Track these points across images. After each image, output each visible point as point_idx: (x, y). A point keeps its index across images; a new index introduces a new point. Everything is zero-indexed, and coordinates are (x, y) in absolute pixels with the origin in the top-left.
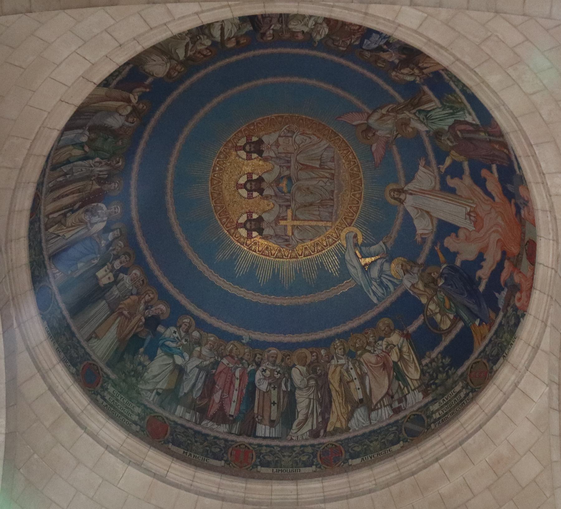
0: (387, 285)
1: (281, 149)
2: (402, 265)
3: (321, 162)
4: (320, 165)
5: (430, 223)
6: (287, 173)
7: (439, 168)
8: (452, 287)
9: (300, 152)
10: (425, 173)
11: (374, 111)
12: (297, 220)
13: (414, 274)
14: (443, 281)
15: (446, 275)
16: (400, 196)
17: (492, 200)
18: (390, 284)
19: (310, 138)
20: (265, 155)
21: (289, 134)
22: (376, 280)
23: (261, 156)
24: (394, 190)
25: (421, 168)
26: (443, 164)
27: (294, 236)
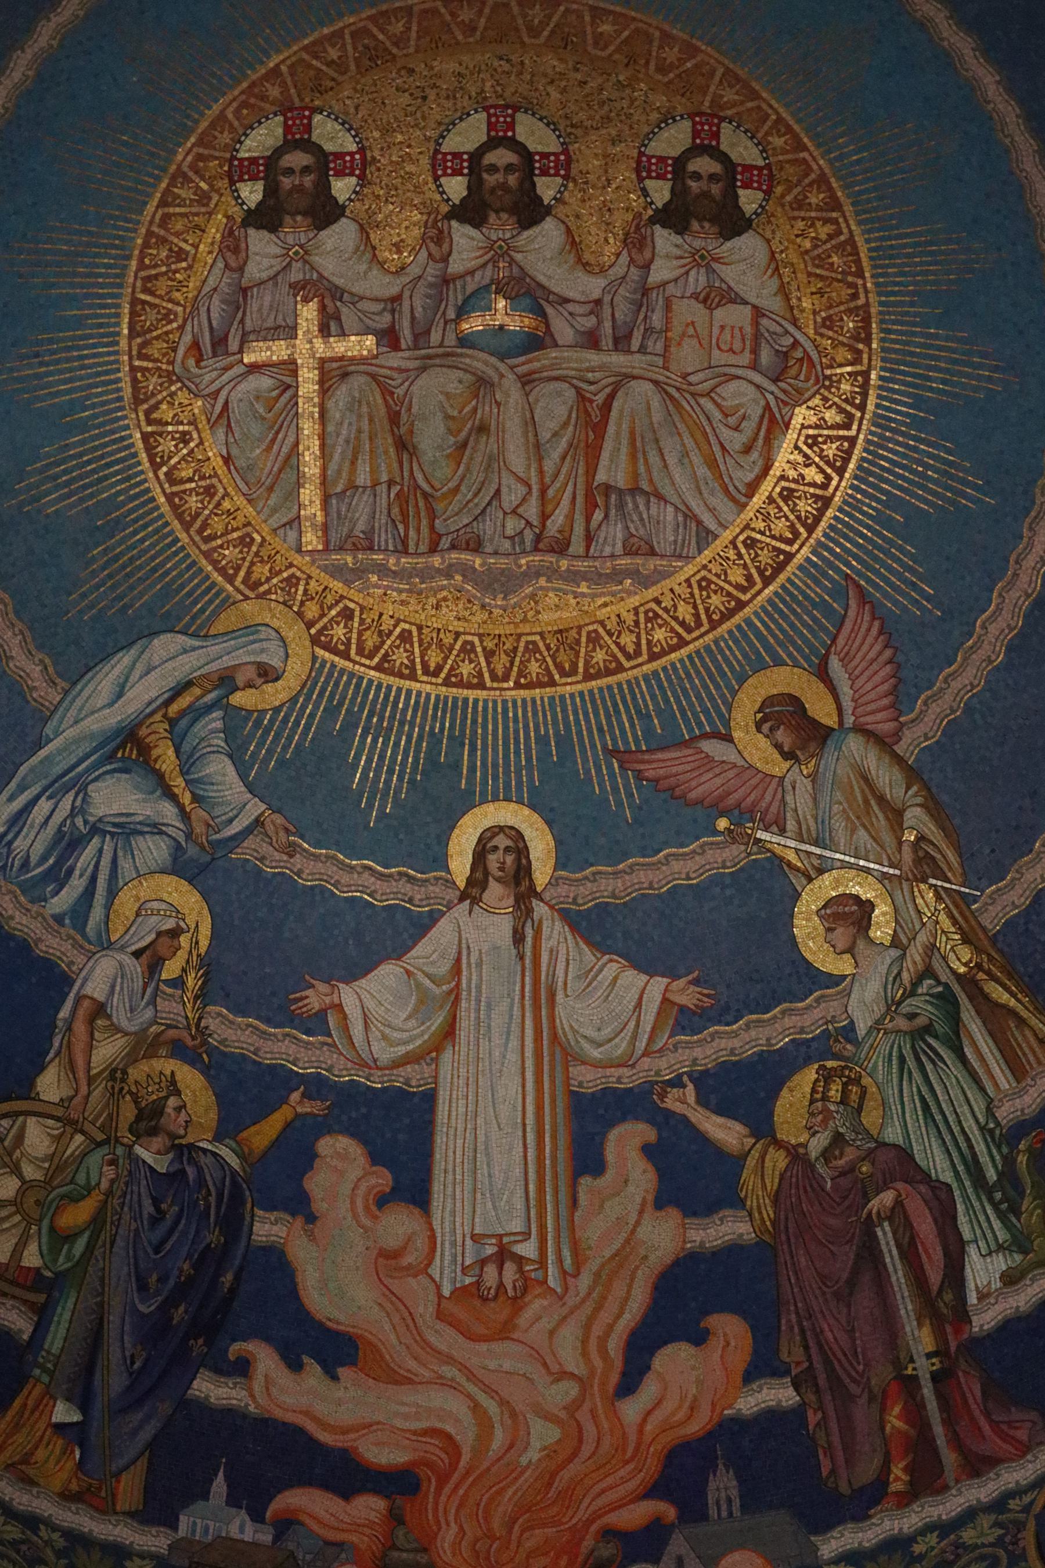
0: (70, 872)
1: (688, 311)
2: (175, 933)
3: (620, 492)
4: (607, 489)
5: (402, 1050)
6: (563, 330)
7: (677, 1082)
8: (155, 1221)
9: (671, 398)
10: (639, 1004)
11: (912, 774)
12: (321, 382)
13: (153, 1002)
14: (162, 1165)
15: (191, 1172)
16: (498, 880)
17: (614, 1378)
18: (77, 885)
19: (747, 450)
20: (664, 239)
21: (766, 357)
22: (83, 811)
23: (652, 221)
24: (520, 848)
25: (659, 983)
26: (702, 1101)
27: (244, 376)
